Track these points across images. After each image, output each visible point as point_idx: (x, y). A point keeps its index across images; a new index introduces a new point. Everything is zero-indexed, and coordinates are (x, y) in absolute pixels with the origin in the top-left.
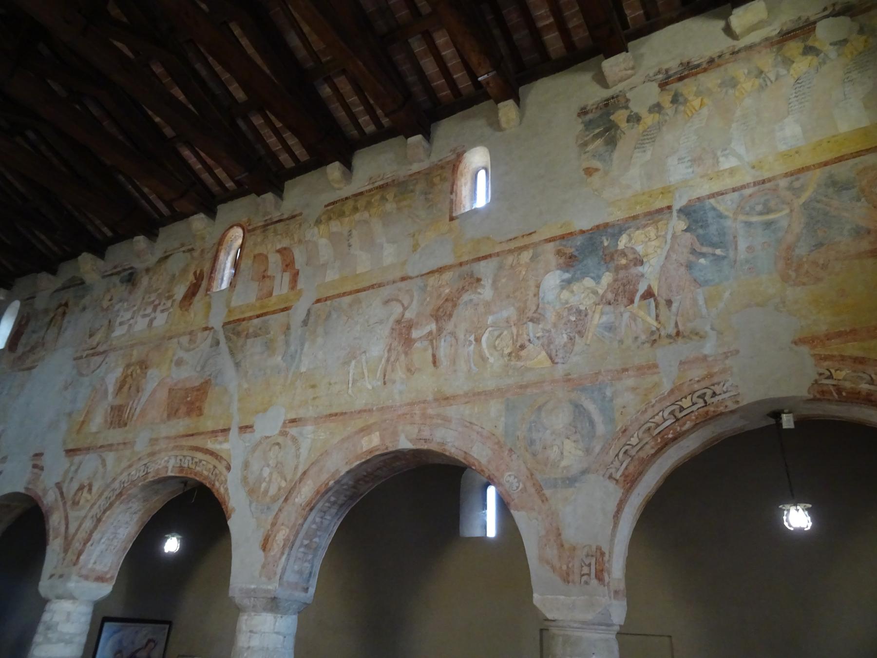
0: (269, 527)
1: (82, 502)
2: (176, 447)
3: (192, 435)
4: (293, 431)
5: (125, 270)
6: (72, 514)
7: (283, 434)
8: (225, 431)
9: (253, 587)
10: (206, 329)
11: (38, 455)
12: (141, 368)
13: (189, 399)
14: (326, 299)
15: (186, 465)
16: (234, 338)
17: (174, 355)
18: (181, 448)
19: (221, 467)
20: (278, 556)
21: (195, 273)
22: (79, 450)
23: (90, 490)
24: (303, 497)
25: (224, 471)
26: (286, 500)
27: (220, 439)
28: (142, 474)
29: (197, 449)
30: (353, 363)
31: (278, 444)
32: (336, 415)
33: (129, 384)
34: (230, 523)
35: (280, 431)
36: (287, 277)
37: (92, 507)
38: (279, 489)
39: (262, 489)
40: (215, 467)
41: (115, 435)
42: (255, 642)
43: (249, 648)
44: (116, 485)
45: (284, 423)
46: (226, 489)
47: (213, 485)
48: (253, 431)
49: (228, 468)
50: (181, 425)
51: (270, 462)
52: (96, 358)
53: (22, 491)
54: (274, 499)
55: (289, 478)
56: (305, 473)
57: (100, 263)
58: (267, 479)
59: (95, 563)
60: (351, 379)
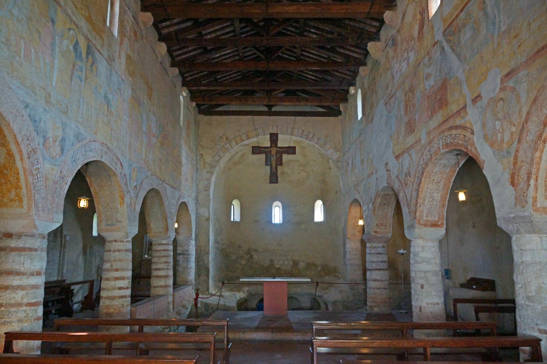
0: (512, 167)
1: (408, 182)
4: (511, 84)
5: (389, 40)
6: (406, 191)
7: (502, 89)
8: (465, 107)
9: (512, 216)
10: (435, 44)
11: (387, 164)
12: (412, 93)
13: (438, 97)
18: (443, 132)
19: (468, 134)
20: (525, 188)
21: (420, 12)
22: (400, 154)
23: (410, 176)
24: (533, 133)
26: (519, 141)
27: (462, 115)
28: (429, 157)
29: (451, 128)
31: (502, 99)
34: (484, 172)
35: (501, 89)
37: (413, 184)
38: (512, 135)
39: (499, 139)
40: (465, 136)
41: (411, 140)
43: (523, 262)
45: (502, 80)
46: (476, 149)
47: (467, 149)
48: (482, 98)
49: (473, 133)
50: (439, 117)
52: (392, 99)
54: (510, 144)
55: (516, 124)
56: (528, 113)
57: (378, 43)
58: (501, 130)
59: (427, 216)
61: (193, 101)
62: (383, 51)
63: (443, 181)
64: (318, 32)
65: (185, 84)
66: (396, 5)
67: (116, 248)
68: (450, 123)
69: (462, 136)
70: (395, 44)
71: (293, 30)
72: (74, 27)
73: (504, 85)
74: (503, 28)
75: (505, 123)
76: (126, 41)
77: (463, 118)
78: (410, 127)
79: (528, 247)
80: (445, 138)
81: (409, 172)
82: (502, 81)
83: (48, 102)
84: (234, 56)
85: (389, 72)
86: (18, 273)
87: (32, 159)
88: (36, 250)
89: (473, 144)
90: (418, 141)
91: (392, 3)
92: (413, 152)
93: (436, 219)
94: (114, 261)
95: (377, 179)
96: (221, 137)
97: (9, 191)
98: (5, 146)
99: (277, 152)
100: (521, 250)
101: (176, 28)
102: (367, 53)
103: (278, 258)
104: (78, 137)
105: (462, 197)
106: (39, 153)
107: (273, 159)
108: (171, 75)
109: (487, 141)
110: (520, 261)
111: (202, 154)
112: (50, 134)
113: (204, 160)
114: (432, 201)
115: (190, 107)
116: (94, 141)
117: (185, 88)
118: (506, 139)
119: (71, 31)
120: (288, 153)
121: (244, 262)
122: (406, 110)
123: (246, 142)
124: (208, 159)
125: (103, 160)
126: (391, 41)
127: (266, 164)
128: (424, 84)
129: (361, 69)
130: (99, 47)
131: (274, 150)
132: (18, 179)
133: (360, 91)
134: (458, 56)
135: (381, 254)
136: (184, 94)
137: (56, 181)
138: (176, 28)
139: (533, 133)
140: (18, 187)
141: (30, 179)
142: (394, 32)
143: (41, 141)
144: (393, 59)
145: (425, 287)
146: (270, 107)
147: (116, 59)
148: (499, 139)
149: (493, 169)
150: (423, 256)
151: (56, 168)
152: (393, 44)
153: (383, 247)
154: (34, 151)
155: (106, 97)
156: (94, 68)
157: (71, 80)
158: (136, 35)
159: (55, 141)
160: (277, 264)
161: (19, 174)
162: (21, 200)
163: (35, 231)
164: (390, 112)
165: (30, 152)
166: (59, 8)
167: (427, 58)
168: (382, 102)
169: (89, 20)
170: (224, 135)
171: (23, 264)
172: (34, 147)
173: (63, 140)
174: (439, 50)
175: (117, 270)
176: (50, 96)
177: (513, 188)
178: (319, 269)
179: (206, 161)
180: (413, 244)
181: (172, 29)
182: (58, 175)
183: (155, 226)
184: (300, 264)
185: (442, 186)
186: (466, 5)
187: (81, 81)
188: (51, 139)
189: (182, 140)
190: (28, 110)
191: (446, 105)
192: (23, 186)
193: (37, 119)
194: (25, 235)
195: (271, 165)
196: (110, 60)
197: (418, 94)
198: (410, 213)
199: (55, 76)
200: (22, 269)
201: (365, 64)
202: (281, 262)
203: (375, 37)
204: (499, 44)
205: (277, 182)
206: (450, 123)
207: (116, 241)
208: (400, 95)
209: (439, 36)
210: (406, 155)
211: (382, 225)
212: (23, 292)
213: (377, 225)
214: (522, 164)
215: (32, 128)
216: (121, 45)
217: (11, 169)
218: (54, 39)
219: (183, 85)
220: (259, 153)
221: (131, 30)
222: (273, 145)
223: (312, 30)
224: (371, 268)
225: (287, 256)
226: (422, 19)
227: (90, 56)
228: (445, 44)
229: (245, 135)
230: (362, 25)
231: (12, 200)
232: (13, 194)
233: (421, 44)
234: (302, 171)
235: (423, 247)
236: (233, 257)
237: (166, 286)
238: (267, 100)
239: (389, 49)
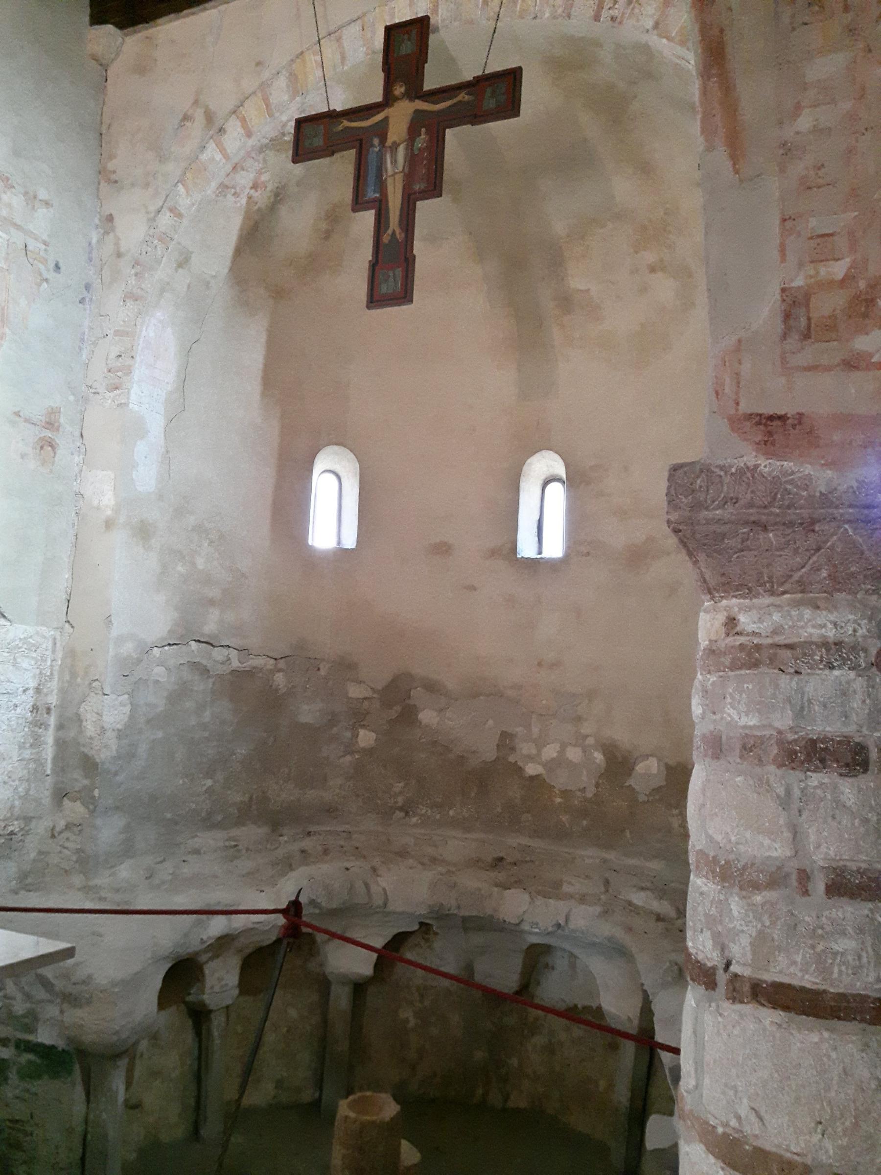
96: (186, 118)
99: (417, 122)
103: (535, 730)
107: (395, 165)
113: (117, 244)
120: (477, 117)
121: (366, 738)
124: (132, 231)
127: (358, 203)
131: (400, 116)
160: (530, 758)
170: (196, 102)
179: (122, 250)
184: (640, 768)
202: (550, 752)
205: (405, 296)
225: (579, 719)
229: (282, 82)
236: (308, 712)
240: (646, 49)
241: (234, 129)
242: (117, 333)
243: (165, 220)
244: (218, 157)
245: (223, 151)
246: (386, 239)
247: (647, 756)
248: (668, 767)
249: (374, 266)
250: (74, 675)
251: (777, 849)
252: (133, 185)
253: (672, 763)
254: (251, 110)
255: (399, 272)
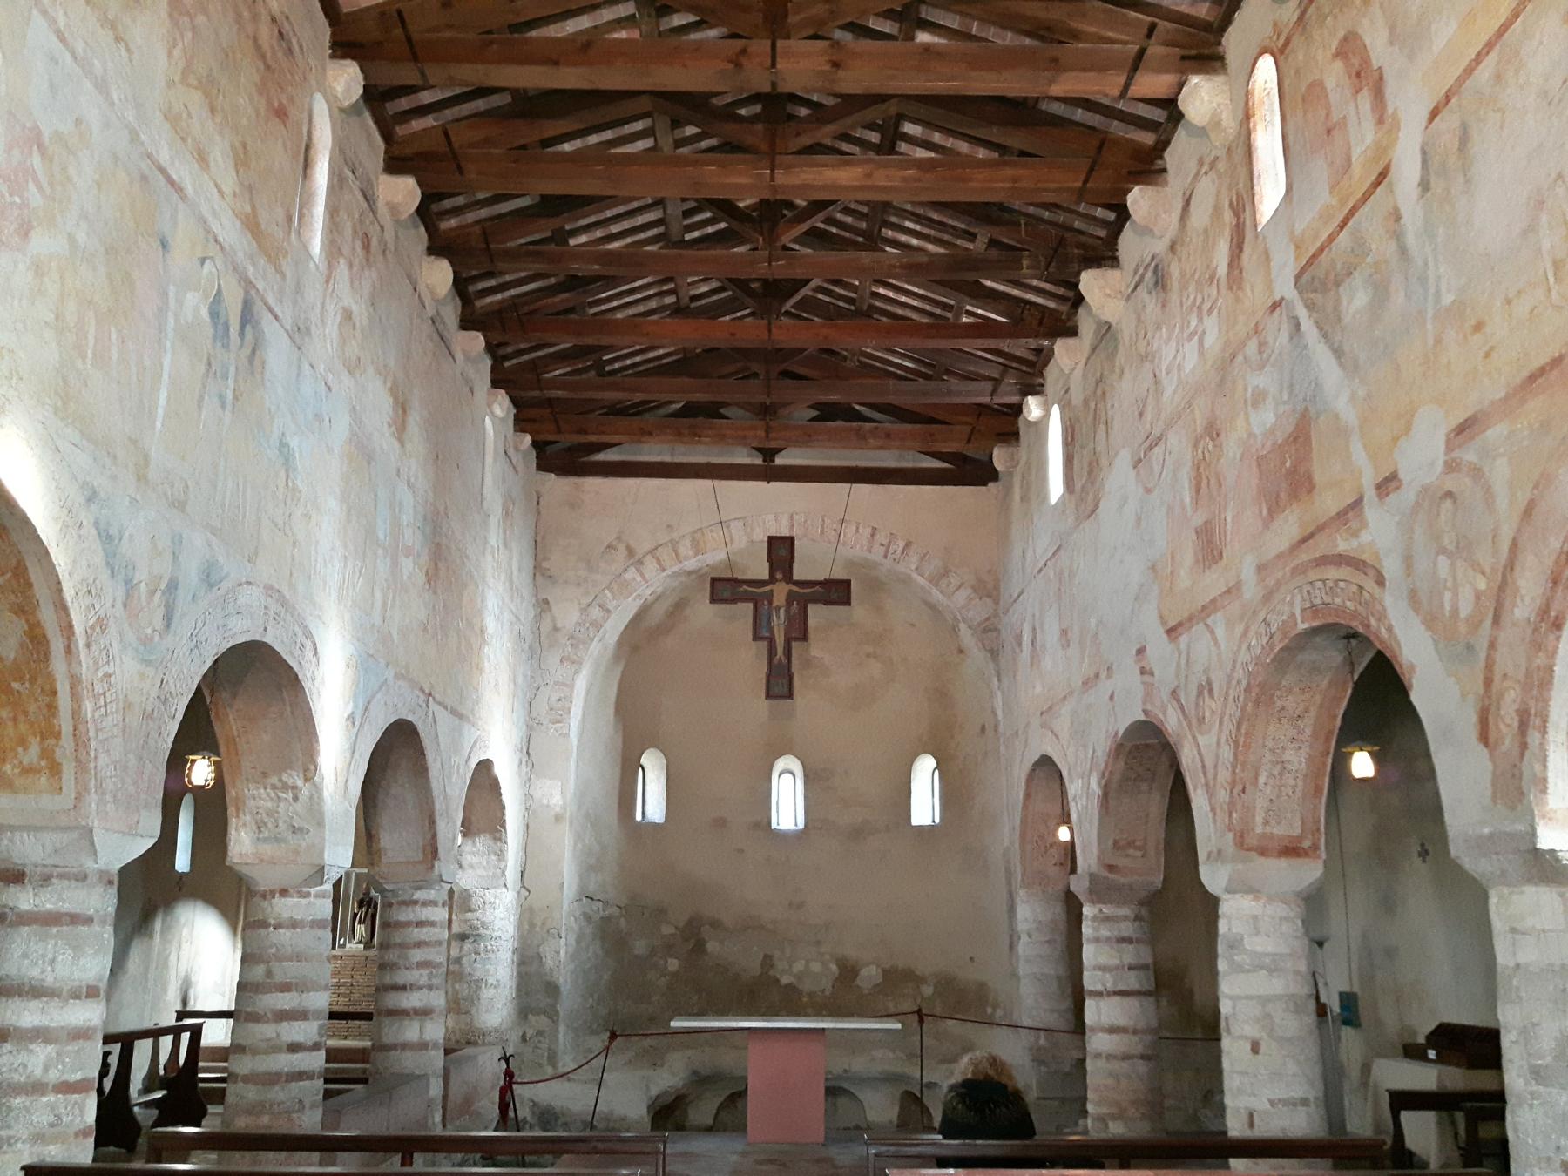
1: (1207, 714)
2: (1300, 570)
3: (1311, 536)
4: (1469, 455)
5: (1146, 268)
6: (1201, 740)
7: (1451, 467)
8: (1357, 503)
9: (1486, 831)
10: (1275, 306)
12: (1212, 439)
14: (1448, 99)
15: (1318, 601)
16: (1317, 298)
17: (1245, 389)
20: (1516, 751)
21: (1231, 204)
22: (1180, 624)
23: (1211, 691)
24: (1527, 600)
25: (1376, 590)
26: (1496, 621)
27: (1353, 524)
29: (1323, 561)
30: (1544, 218)
31: (1449, 494)
32: (1542, 371)
33: (1203, 479)
35: (1446, 462)
36: (1365, 101)
39: (1447, 607)
40: (1361, 588)
42: (1528, 954)
44: (1240, 674)
45: (1448, 441)
46: (1390, 629)
47: (1368, 626)
49: (1381, 582)
50: (1289, 527)
51: (1446, 542)
52: (1156, 449)
53: (1143, 718)
54: (1475, 625)
55: (1488, 570)
56: (1514, 545)
58: (1449, 584)
59: (1266, 823)
60: (1549, 265)
61: (523, 431)
62: (1128, 299)
63: (1313, 713)
64: (926, 231)
65: (499, 380)
66: (1164, 170)
67: (286, 915)
68: (1321, 547)
69: (1354, 588)
70: (1160, 282)
71: (849, 219)
72: (213, 250)
73: (1454, 455)
74: (1447, 299)
75: (1460, 564)
76: (342, 268)
77: (1356, 534)
78: (1210, 542)
79: (1529, 922)
80: (1307, 587)
81: (1209, 683)
82: (1449, 447)
83: (141, 478)
84: (661, 294)
85: (1148, 365)
86: (36, 991)
87: (94, 648)
88: (89, 921)
89: (1382, 617)
90: (1232, 591)
91: (1152, 163)
92: (1218, 621)
93: (1297, 832)
94: (280, 960)
95: (1111, 697)
96: (610, 547)
97: (23, 742)
98: (24, 612)
99: (791, 597)
100: (1513, 930)
101: (484, 213)
102: (1079, 300)
104: (210, 578)
105: (1362, 765)
106: (113, 629)
107: (779, 621)
108: (459, 356)
109: (1416, 611)
110: (1512, 964)
111: (546, 602)
112: (141, 575)
113: (554, 620)
114: (1281, 774)
115: (511, 452)
116: (249, 583)
117: (502, 395)
118: (1465, 611)
119: (208, 264)
120: (828, 602)
121: (673, 964)
122: (1198, 491)
123: (691, 564)
124: (568, 615)
125: (268, 639)
126: (1149, 274)
127: (757, 637)
128: (1247, 420)
129: (1060, 346)
130: (271, 301)
131: (780, 591)
132: (52, 708)
133: (1056, 411)
134: (1338, 353)
135: (1129, 940)
136: (498, 411)
137: (149, 709)
138: (484, 213)
139: (1527, 600)
140: (49, 733)
141: (88, 706)
142: (1160, 247)
143: (120, 595)
144: (1158, 327)
145: (1263, 1048)
146: (769, 454)
147: (313, 328)
148: (1447, 607)
149: (1436, 694)
150: (1259, 949)
151: (150, 671)
152: (1156, 283)
153: (1137, 918)
154: (102, 624)
155: (283, 445)
156: (257, 362)
157: (200, 407)
158: (367, 246)
159: (152, 593)
161: (55, 693)
162: (55, 769)
163: (90, 865)
164: (1148, 491)
165: (92, 627)
166: (181, 206)
167: (1252, 347)
168: (1123, 460)
169: (251, 225)
171: (53, 962)
172: (101, 613)
173: (173, 586)
174: (1285, 326)
175: (285, 988)
176: (146, 457)
177: (1485, 751)
178: (928, 990)
179: (559, 625)
180: (1224, 909)
181: (471, 217)
182: (154, 694)
183: (396, 842)
184: (864, 972)
185: (1308, 731)
186: (1352, 213)
187: (223, 406)
188: (143, 585)
189: (489, 558)
190: (93, 507)
191: (1310, 492)
192: (66, 727)
193: (113, 531)
194: (61, 876)
195: (771, 641)
196: (299, 333)
197: (1232, 447)
198: (1213, 809)
199: (162, 401)
200: (49, 980)
201: (1073, 332)
202: (799, 966)
203: (1104, 255)
204: (1438, 341)
206: (1321, 547)
207: (284, 892)
208: (1178, 443)
209: (1285, 287)
210: (1199, 628)
211: (1131, 844)
212: (50, 1048)
213: (1115, 843)
214: (1506, 684)
215: (99, 559)
216: (327, 282)
217: (33, 680)
218: (164, 294)
219: (496, 384)
220: (733, 601)
221: (355, 232)
222: (779, 576)
223: (908, 224)
224: (1099, 988)
225: (818, 943)
226: (1237, 225)
227: (248, 328)
228: (1302, 313)
229: (688, 542)
230: (1061, 218)
231: (28, 771)
232: (32, 754)
233: (1238, 300)
234: (868, 656)
235: (1255, 918)
236: (640, 947)
237: (423, 1046)
238: (762, 433)
239: (1146, 297)
240: (909, 577)
241: (650, 566)
242: (556, 683)
243: (596, 613)
244: (639, 579)
245: (643, 577)
246: (776, 661)
247: (868, 965)
248: (884, 971)
249: (769, 677)
250: (532, 925)
251: (1117, 962)
252: (566, 582)
253: (887, 966)
254: (665, 554)
255: (786, 682)
